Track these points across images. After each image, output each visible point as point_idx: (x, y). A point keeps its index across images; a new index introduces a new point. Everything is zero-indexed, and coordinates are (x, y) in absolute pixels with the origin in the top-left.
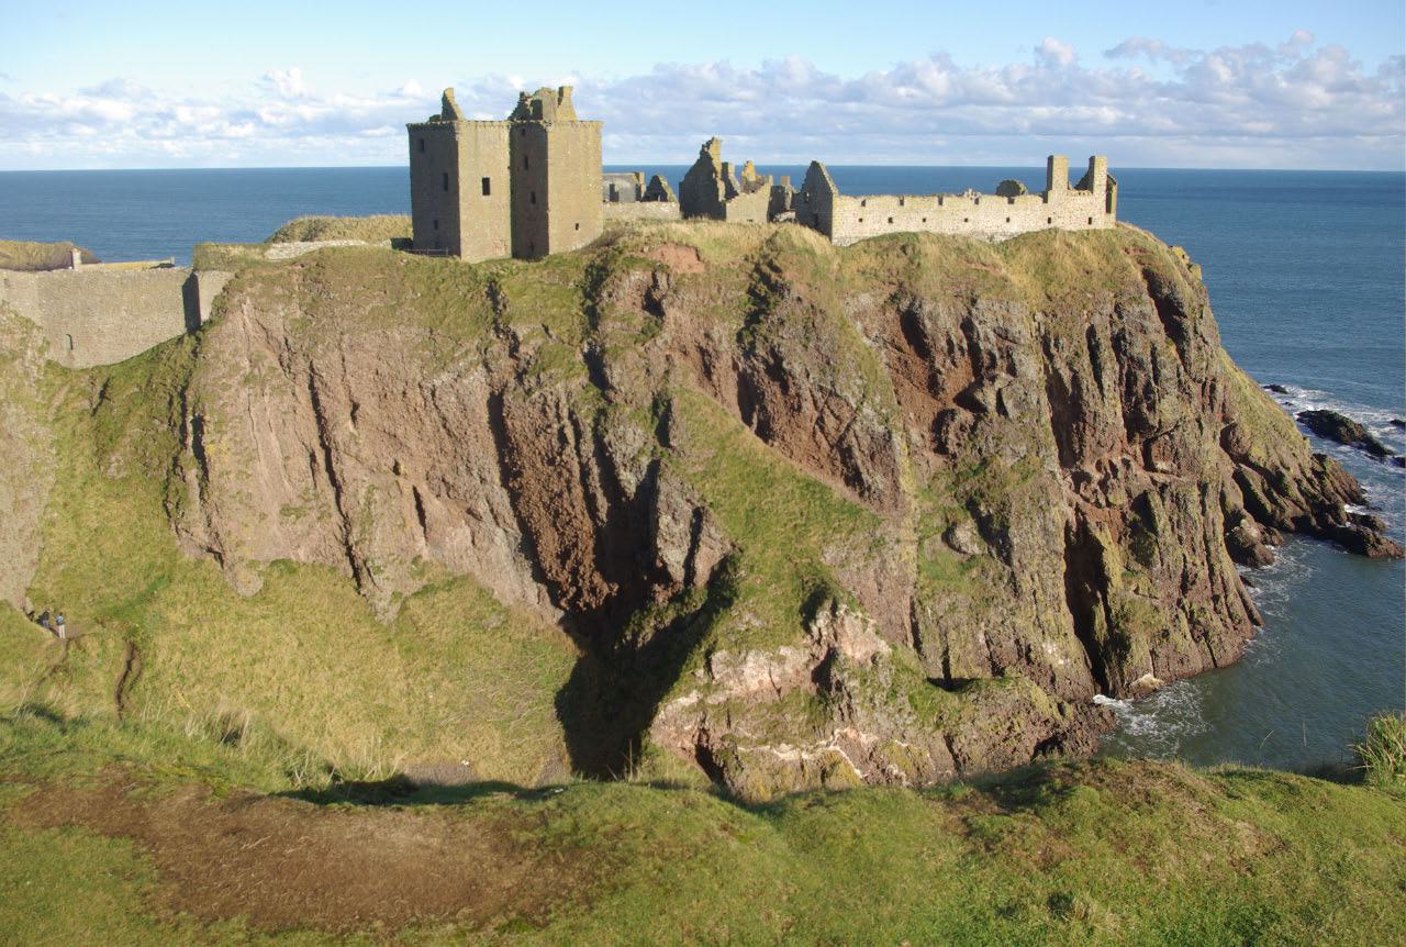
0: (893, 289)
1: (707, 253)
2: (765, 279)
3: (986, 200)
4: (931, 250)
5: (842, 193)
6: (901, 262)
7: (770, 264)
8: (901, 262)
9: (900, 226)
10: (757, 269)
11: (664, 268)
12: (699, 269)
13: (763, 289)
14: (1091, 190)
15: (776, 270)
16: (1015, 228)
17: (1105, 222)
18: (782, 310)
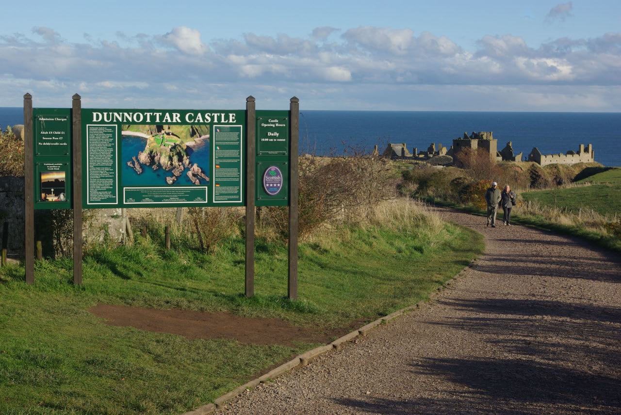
0: (555, 177)
1: (523, 169)
2: (533, 174)
3: (568, 155)
4: (561, 167)
5: (542, 154)
6: (556, 171)
7: (535, 171)
8: (556, 171)
9: (554, 162)
10: (531, 172)
11: (517, 172)
12: (522, 172)
13: (534, 176)
14: (588, 152)
15: (537, 172)
16: (574, 162)
17: (591, 161)
18: (540, 181)
